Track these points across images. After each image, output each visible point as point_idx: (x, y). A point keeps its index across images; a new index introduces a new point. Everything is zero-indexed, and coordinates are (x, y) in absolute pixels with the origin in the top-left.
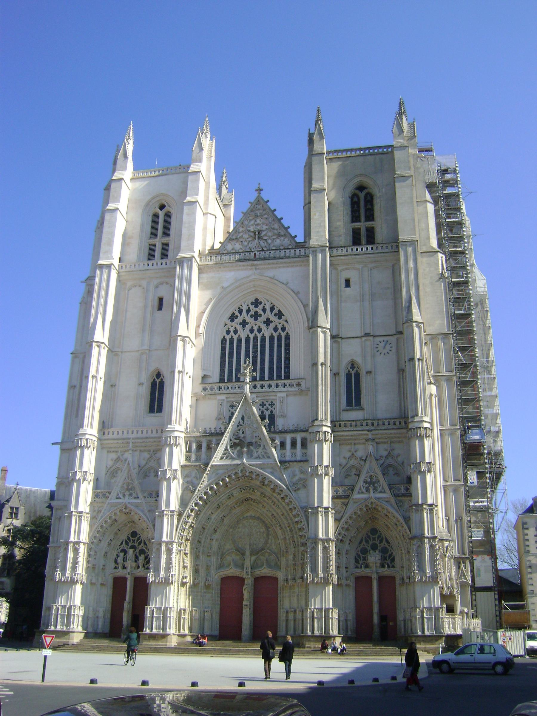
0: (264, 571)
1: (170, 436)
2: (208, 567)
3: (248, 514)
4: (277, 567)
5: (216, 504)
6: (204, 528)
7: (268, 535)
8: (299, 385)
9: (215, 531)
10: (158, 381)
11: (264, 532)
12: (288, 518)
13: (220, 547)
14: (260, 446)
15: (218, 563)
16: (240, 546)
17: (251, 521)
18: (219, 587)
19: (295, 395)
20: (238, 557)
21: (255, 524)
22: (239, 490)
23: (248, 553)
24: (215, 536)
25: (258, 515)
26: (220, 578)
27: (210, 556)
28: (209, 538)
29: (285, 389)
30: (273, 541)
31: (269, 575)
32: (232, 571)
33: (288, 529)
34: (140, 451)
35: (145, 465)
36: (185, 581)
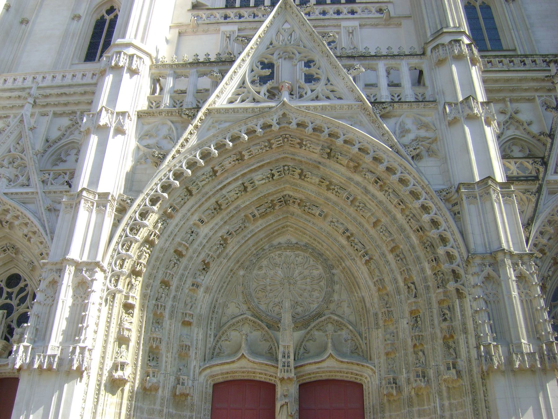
0: (329, 366)
1: (120, 53)
2: (183, 351)
3: (282, 239)
4: (361, 353)
5: (213, 200)
6: (179, 254)
7: (331, 282)
8: (380, 11)
9: (206, 267)
10: (108, 18)
11: (320, 278)
12: (393, 230)
13: (213, 309)
14: (318, 80)
15: (209, 345)
16: (263, 307)
17: (288, 253)
18: (209, 406)
19: (375, 26)
20: (257, 334)
21: (299, 259)
22: (266, 172)
23: (287, 319)
24: (206, 280)
25: (306, 240)
26: (211, 382)
27: (189, 324)
28: (189, 282)
29: (356, 16)
30: (344, 296)
31: (339, 376)
32: (243, 363)
33: (390, 257)
34: (55, 114)
35: (60, 139)
36: (118, 374)
